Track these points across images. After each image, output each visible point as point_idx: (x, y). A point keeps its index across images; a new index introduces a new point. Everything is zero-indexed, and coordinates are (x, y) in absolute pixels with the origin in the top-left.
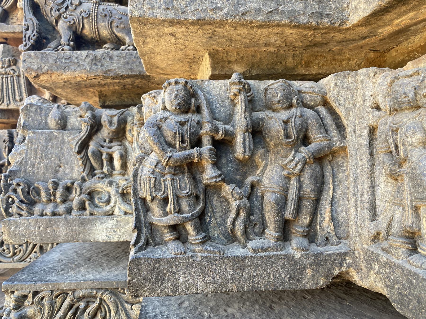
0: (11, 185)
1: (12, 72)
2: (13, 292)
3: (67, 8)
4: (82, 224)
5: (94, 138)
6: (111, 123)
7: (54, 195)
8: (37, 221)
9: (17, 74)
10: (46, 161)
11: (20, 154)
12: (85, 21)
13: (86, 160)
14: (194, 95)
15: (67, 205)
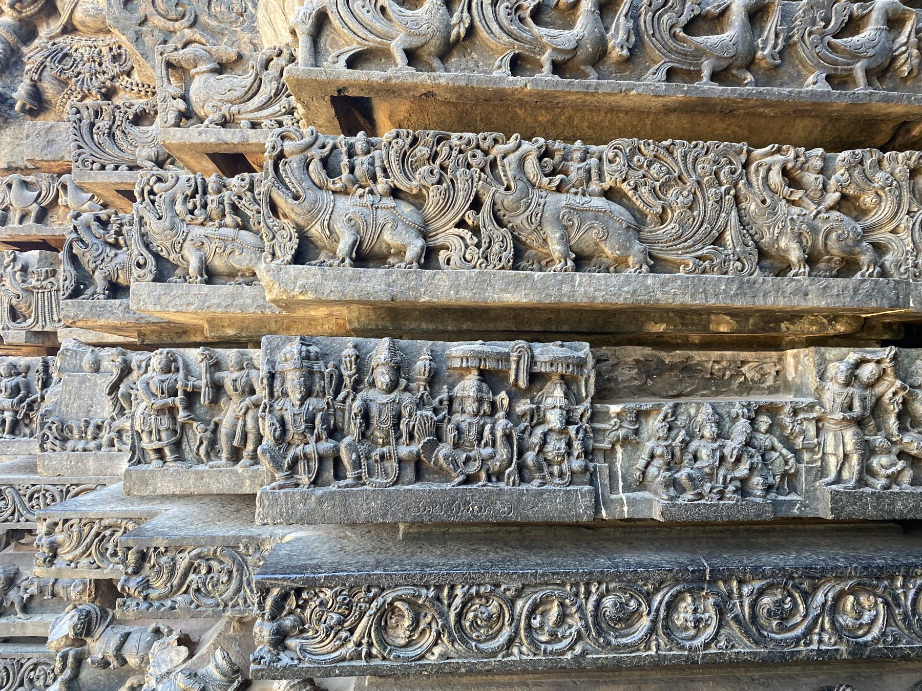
0: (46, 423)
1: (49, 285)
2: (45, 520)
3: (102, 261)
4: (110, 459)
5: (125, 380)
6: (139, 367)
7: (86, 433)
8: (69, 456)
9: (55, 288)
10: (79, 402)
11: (56, 395)
12: (120, 272)
13: (116, 401)
14: (175, 360)
15: (97, 442)
